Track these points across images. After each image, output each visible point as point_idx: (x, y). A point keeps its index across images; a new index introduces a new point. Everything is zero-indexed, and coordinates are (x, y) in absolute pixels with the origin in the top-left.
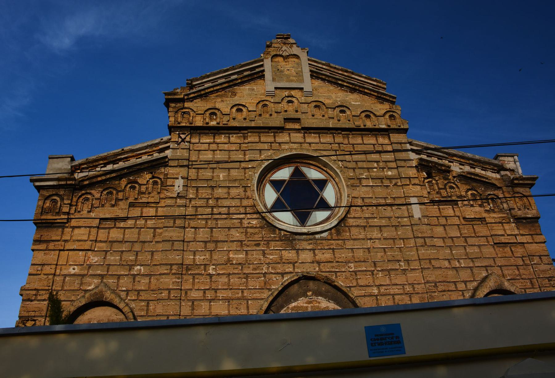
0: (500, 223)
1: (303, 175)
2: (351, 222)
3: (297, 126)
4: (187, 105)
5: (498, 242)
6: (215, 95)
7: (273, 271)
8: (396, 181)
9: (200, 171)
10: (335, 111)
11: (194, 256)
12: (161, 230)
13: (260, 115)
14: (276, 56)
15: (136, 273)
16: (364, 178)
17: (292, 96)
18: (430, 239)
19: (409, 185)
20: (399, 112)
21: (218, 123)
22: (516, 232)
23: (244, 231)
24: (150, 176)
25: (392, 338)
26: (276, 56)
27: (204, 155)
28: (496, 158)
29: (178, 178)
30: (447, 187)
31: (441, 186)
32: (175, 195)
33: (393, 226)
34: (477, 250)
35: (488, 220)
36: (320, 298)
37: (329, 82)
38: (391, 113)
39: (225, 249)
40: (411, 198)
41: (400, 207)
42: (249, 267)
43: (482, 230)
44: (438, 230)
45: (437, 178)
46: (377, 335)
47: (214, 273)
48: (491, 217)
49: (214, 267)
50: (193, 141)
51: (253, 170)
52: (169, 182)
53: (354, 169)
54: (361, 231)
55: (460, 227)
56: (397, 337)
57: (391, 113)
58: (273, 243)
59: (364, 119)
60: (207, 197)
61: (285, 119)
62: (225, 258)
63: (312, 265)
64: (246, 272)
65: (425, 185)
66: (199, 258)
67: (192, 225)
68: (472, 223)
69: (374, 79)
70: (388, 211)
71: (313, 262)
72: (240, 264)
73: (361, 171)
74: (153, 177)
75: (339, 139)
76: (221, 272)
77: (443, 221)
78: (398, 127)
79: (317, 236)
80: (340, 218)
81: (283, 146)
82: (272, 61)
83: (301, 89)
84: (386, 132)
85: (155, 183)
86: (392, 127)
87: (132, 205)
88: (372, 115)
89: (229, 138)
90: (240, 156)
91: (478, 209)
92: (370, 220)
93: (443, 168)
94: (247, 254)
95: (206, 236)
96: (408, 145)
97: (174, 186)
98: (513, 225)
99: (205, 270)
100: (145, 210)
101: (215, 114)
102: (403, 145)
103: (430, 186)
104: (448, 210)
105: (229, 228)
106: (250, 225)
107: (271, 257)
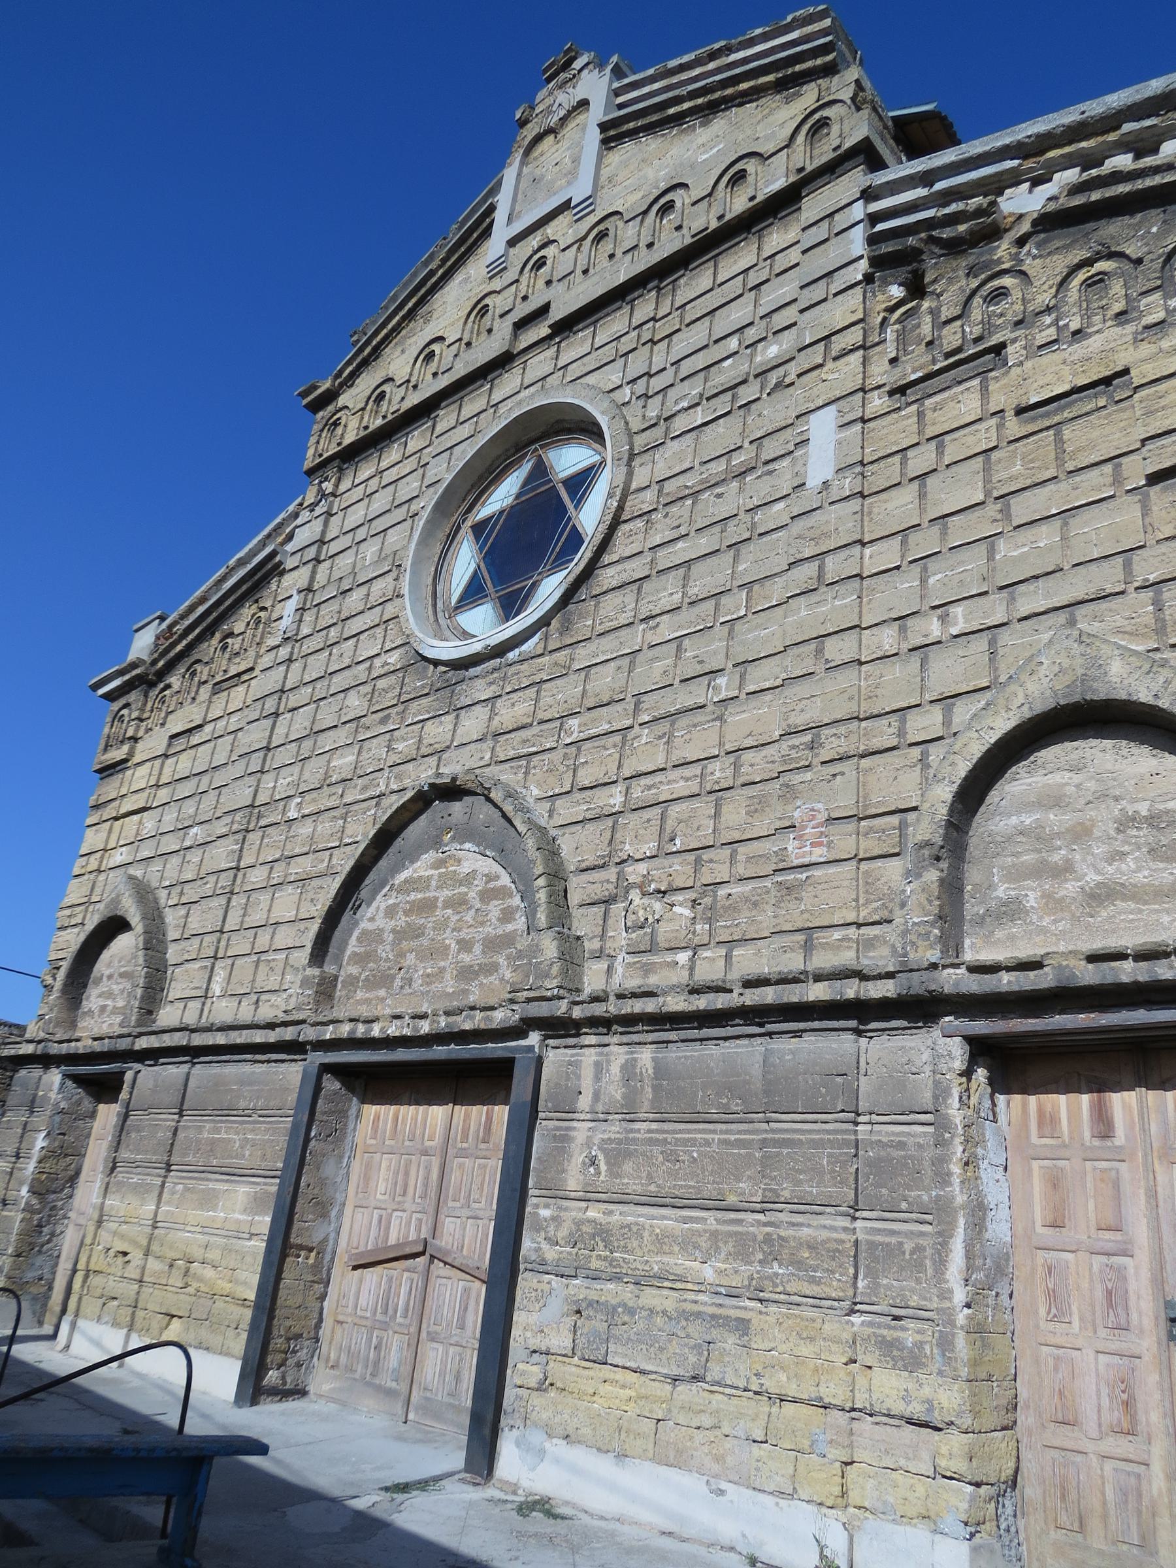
2: (608, 577)
4: (342, 400)
13: (468, 344)
14: (538, 138)
21: (384, 417)
36: (467, 846)
37: (649, 129)
41: (770, 467)
44: (890, 506)
49: (299, 800)
61: (515, 324)
69: (789, 18)
75: (645, 307)
79: (512, 655)
81: (503, 408)
93: (962, 228)
104: (962, 402)
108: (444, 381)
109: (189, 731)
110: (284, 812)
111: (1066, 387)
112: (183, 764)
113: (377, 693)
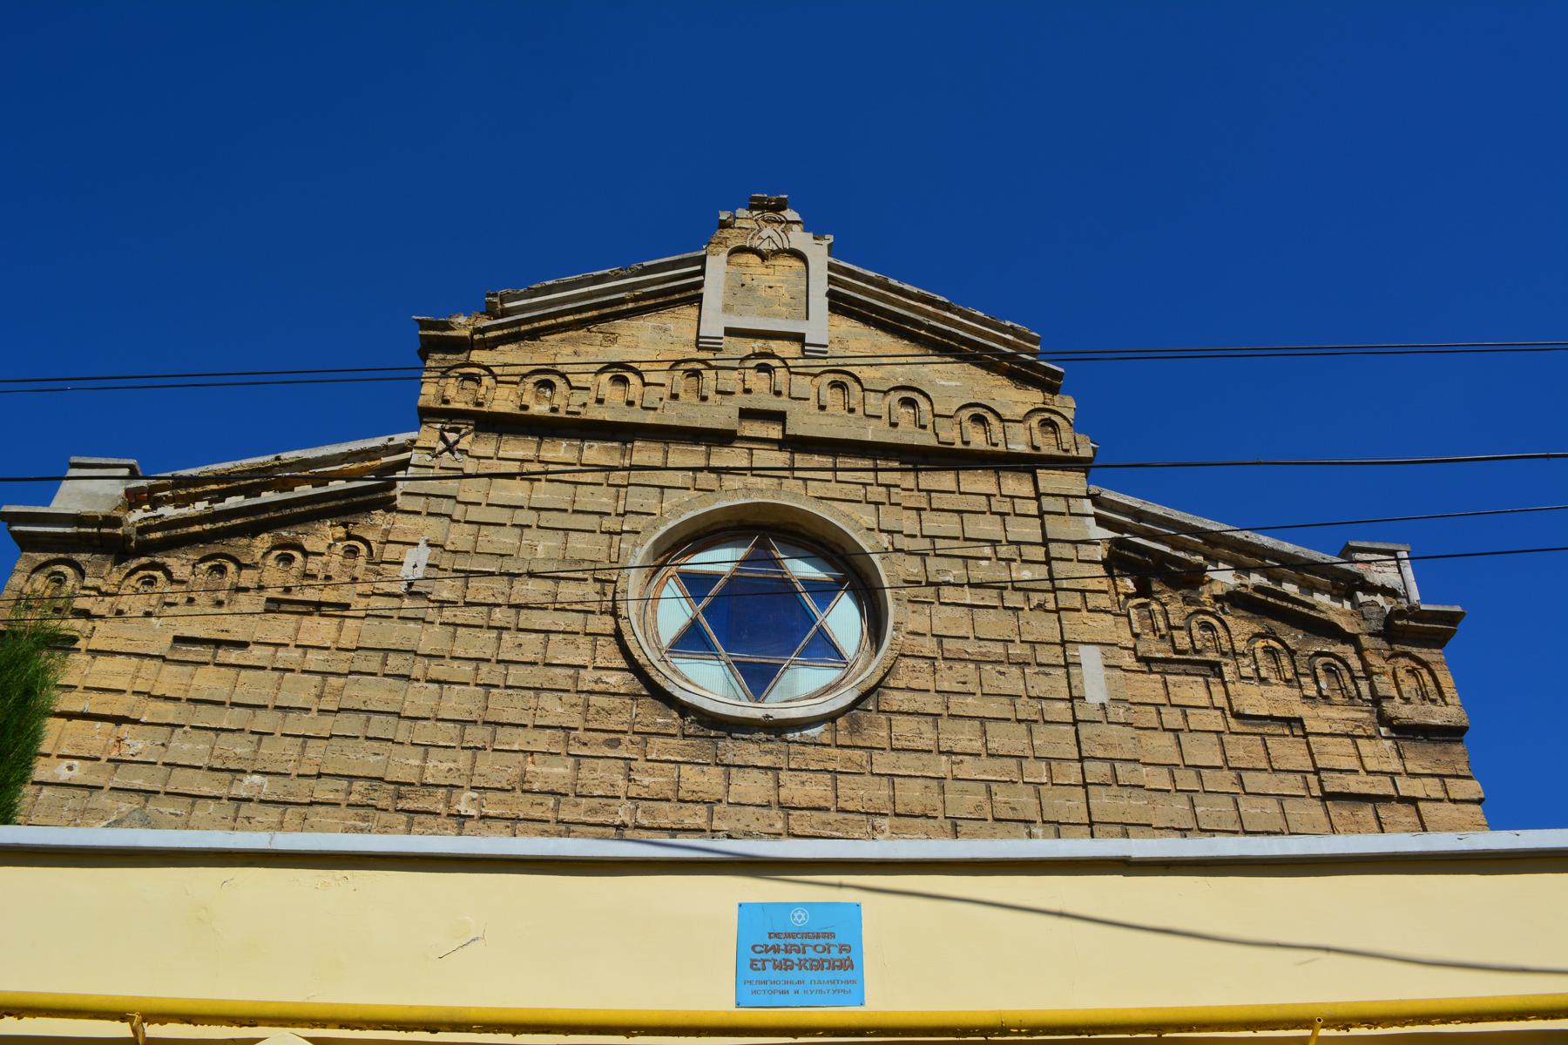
0: (1347, 735)
1: (776, 562)
2: (895, 700)
3: (774, 432)
4: (477, 356)
5: (1338, 790)
6: (558, 336)
7: (645, 822)
8: (1041, 596)
9: (485, 530)
10: (888, 398)
11: (425, 760)
12: (343, 680)
14: (741, 250)
15: (244, 795)
16: (948, 584)
17: (772, 356)
18: (1132, 766)
19: (1079, 610)
20: (1070, 415)
21: (554, 410)
22: (1395, 765)
23: (580, 701)
24: (340, 532)
25: (827, 949)
26: (741, 250)
27: (505, 488)
28: (1347, 552)
29: (416, 544)
30: (1193, 624)
31: (1174, 621)
32: (401, 588)
33: (1019, 721)
34: (1272, 806)
35: (1311, 726)
38: (1047, 415)
39: (516, 747)
40: (1081, 647)
41: (1047, 670)
42: (577, 805)
43: (1290, 752)
44: (1156, 743)
45: (1164, 598)
46: (777, 935)
47: (473, 812)
48: (1318, 718)
49: (475, 795)
50: (479, 450)
51: (633, 537)
52: (391, 552)
53: (923, 555)
54: (924, 727)
55: (1226, 738)
56: (843, 948)
57: (1047, 415)
58: (657, 742)
59: (967, 424)
60: (491, 600)
61: (741, 410)
62: (514, 772)
63: (765, 811)
64: (567, 818)
65: (1128, 615)
66: (438, 768)
67: (433, 674)
68: (1261, 730)
69: (1008, 323)
70: (1012, 681)
71: (768, 806)
72: (552, 793)
73: (944, 563)
74: (349, 537)
76: (491, 813)
77: (1173, 718)
78: (1061, 453)
80: (865, 687)
82: (728, 263)
83: (799, 338)
84: (1028, 464)
85: (352, 552)
86: (1045, 450)
87: (275, 606)
88: (990, 417)
89: (581, 450)
90: (604, 500)
91: (1281, 691)
92: (954, 699)
94: (578, 767)
95: (467, 706)
96: (1088, 502)
97: (401, 563)
98: (1389, 743)
99: (448, 803)
100: (307, 621)
101: (550, 385)
102: (1071, 501)
103: (1141, 618)
104: (1190, 689)
105: (538, 690)
106: (601, 687)
107: (646, 781)
108: (650, 418)
109: (218, 644)
110: (448, 803)
111: (1264, 713)
112: (208, 681)
113: (592, 710)
